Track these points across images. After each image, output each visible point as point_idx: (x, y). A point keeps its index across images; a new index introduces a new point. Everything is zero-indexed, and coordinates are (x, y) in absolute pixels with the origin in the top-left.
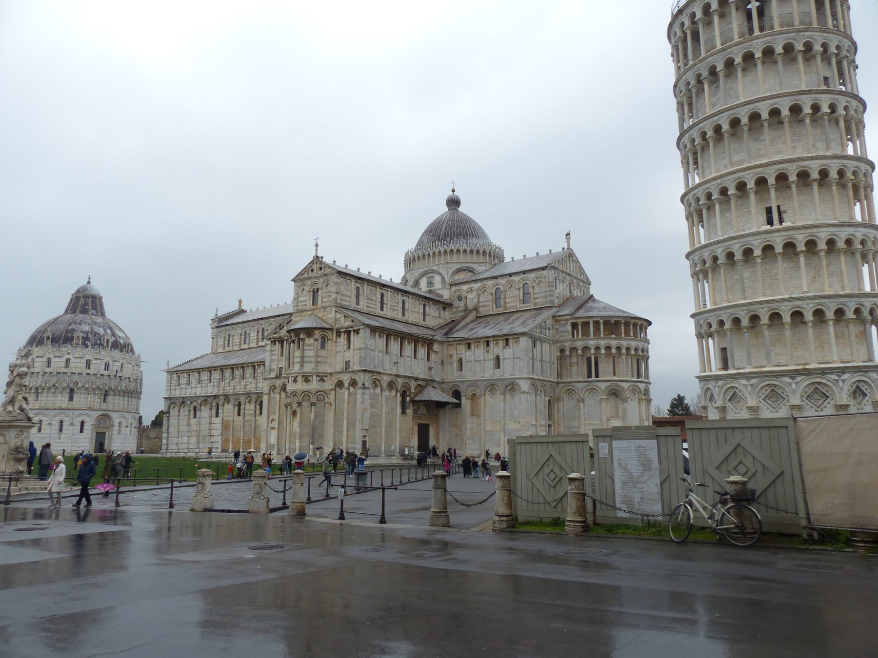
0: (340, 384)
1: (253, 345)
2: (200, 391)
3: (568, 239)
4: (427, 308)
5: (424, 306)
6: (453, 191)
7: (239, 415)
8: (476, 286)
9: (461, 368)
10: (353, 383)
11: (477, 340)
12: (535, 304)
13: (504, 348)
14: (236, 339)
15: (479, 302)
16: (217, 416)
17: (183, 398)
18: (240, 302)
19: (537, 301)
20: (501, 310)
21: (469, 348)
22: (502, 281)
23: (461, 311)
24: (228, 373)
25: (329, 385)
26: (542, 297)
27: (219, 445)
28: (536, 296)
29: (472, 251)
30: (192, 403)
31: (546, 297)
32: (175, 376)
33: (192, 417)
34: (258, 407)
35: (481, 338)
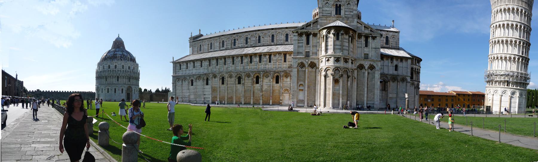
0: (361, 67)
1: (218, 49)
2: (194, 72)
7: (223, 83)
10: (372, 67)
14: (206, 47)
16: (207, 84)
17: (184, 76)
18: (200, 30)
24: (214, 62)
25: (354, 66)
27: (210, 99)
30: (190, 78)
32: (178, 65)
33: (190, 85)
34: (237, 80)
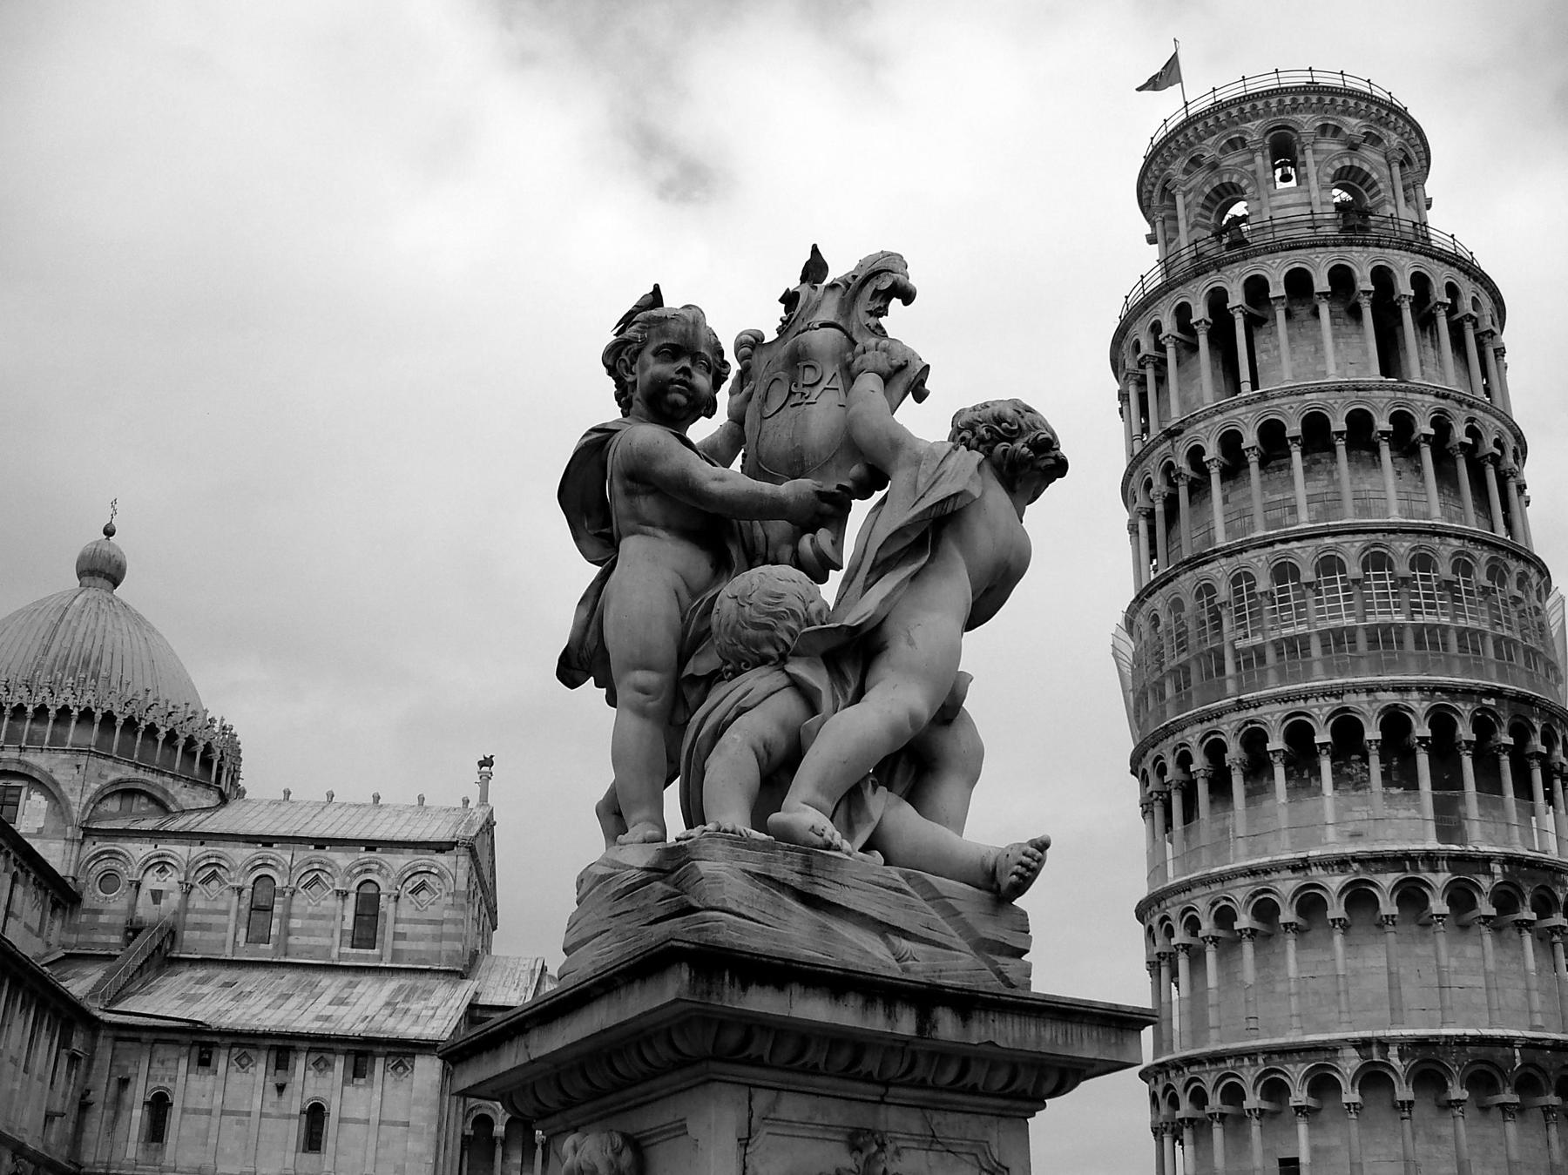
3: (485, 779)
4: (19, 890)
5: (15, 879)
6: (109, 532)
8: (180, 851)
9: (156, 1131)
11: (245, 1042)
12: (396, 954)
13: (345, 1083)
15: (185, 908)
19: (401, 945)
20: (266, 952)
21: (204, 1062)
22: (276, 851)
23: (109, 928)
26: (419, 938)
28: (400, 928)
29: (172, 736)
31: (439, 938)
35: (267, 1035)
